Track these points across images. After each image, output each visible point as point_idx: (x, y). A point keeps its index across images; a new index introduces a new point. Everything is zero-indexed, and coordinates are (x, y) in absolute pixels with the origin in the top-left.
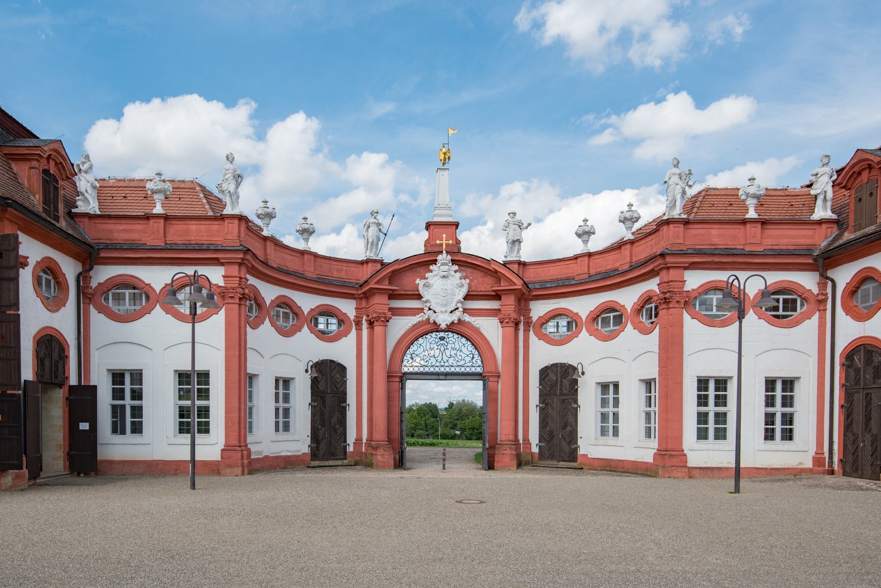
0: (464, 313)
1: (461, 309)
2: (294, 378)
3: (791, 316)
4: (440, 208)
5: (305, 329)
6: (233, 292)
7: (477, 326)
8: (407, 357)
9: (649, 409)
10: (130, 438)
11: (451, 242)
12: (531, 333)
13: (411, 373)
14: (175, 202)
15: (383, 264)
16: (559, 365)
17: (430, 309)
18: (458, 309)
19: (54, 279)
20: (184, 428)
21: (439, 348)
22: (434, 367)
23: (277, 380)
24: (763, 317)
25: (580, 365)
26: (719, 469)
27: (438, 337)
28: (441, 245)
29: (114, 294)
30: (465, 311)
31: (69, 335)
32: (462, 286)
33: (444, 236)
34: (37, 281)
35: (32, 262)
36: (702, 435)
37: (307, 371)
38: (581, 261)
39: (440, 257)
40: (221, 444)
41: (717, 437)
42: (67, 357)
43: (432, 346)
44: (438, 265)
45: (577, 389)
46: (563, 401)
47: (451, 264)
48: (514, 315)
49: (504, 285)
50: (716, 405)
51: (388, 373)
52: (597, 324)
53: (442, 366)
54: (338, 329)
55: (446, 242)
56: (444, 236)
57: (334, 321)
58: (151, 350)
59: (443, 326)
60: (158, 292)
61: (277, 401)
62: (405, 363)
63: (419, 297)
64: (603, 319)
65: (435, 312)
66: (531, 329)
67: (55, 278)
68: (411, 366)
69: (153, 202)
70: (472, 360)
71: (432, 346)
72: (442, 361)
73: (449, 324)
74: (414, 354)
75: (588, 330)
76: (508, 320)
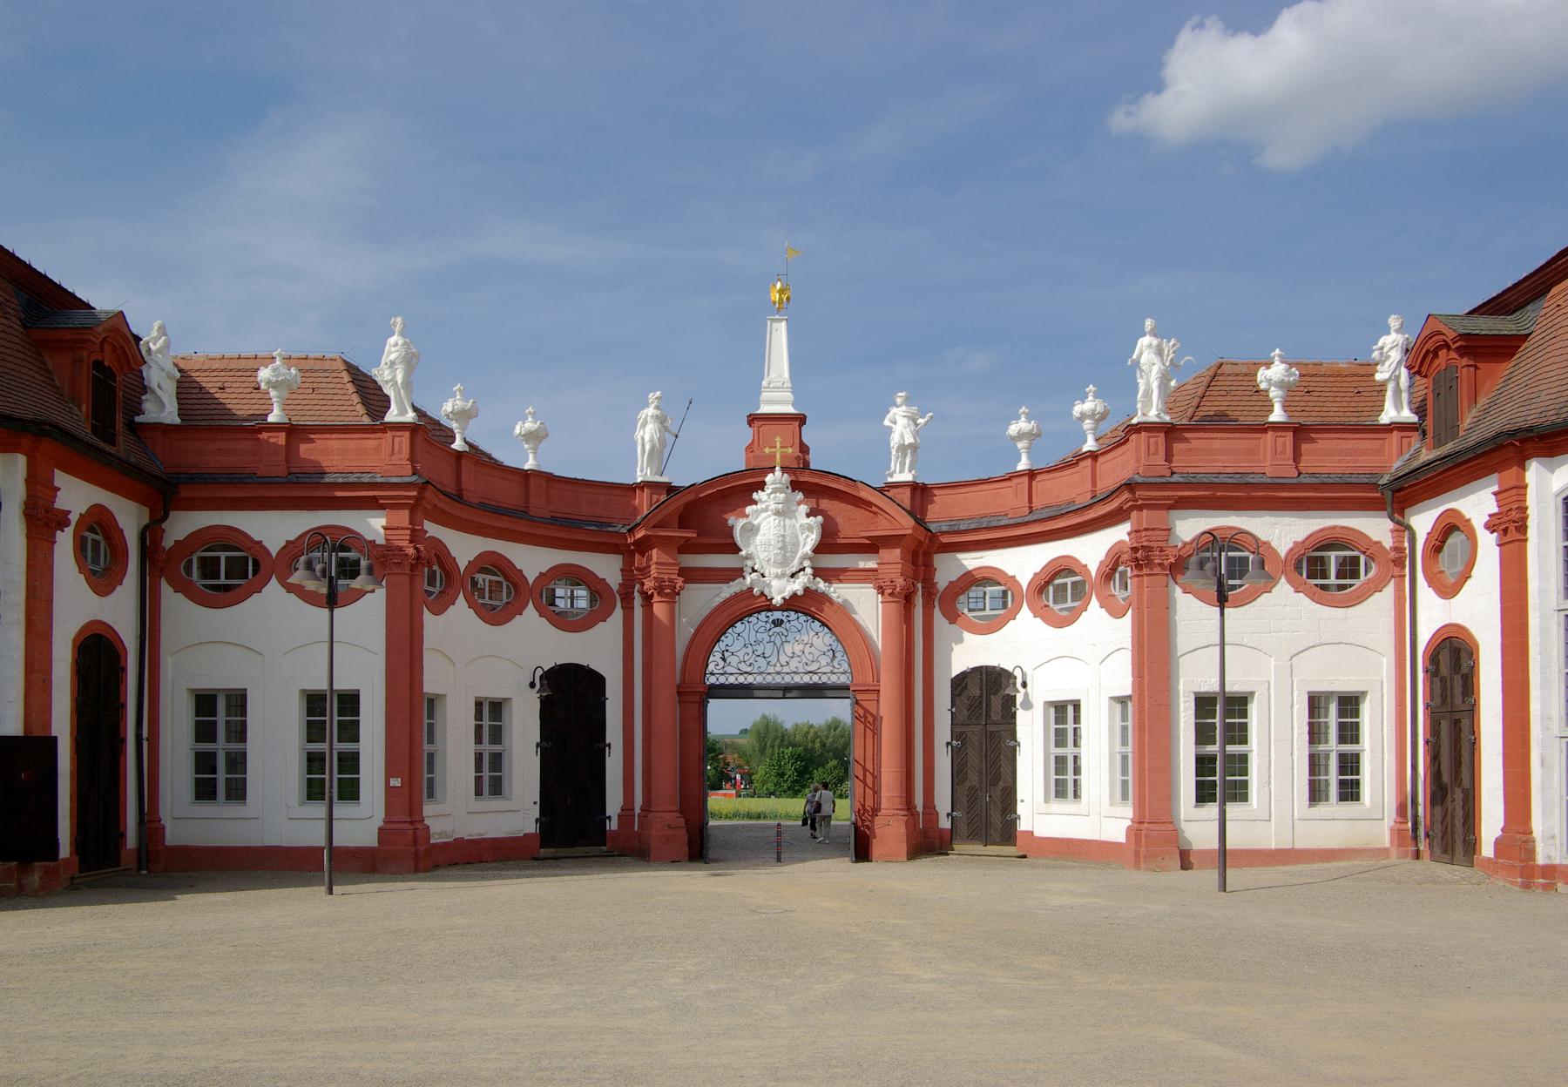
0: (815, 575)
1: (809, 571)
2: (511, 699)
3: (1351, 585)
4: (773, 388)
5: (530, 610)
6: (401, 555)
7: (840, 600)
8: (715, 658)
9: (1124, 749)
10: (221, 809)
12: (937, 613)
13: (722, 686)
14: (304, 396)
15: (670, 489)
16: (984, 671)
17: (754, 571)
18: (803, 569)
19: (105, 539)
20: (314, 791)
21: (773, 637)
22: (764, 675)
24: (1302, 590)
25: (1018, 670)
27: (770, 621)
28: (773, 456)
29: (203, 560)
30: (818, 573)
31: (128, 634)
33: (778, 439)
34: (80, 546)
35: (74, 518)
37: (532, 685)
38: (1018, 484)
39: (769, 478)
40: (379, 817)
42: (124, 670)
43: (760, 637)
44: (769, 491)
45: (1015, 712)
47: (790, 490)
49: (882, 528)
51: (678, 687)
52: (1048, 601)
53: (778, 673)
54: (591, 607)
56: (778, 439)
57: (582, 593)
58: (261, 654)
59: (778, 600)
60: (274, 556)
61: (479, 740)
62: (711, 667)
63: (735, 549)
65: (763, 576)
66: (936, 604)
67: (107, 538)
68: (722, 674)
69: (269, 402)
70: (832, 661)
71: (760, 637)
72: (778, 665)
73: (787, 598)
74: (727, 651)
76: (891, 591)
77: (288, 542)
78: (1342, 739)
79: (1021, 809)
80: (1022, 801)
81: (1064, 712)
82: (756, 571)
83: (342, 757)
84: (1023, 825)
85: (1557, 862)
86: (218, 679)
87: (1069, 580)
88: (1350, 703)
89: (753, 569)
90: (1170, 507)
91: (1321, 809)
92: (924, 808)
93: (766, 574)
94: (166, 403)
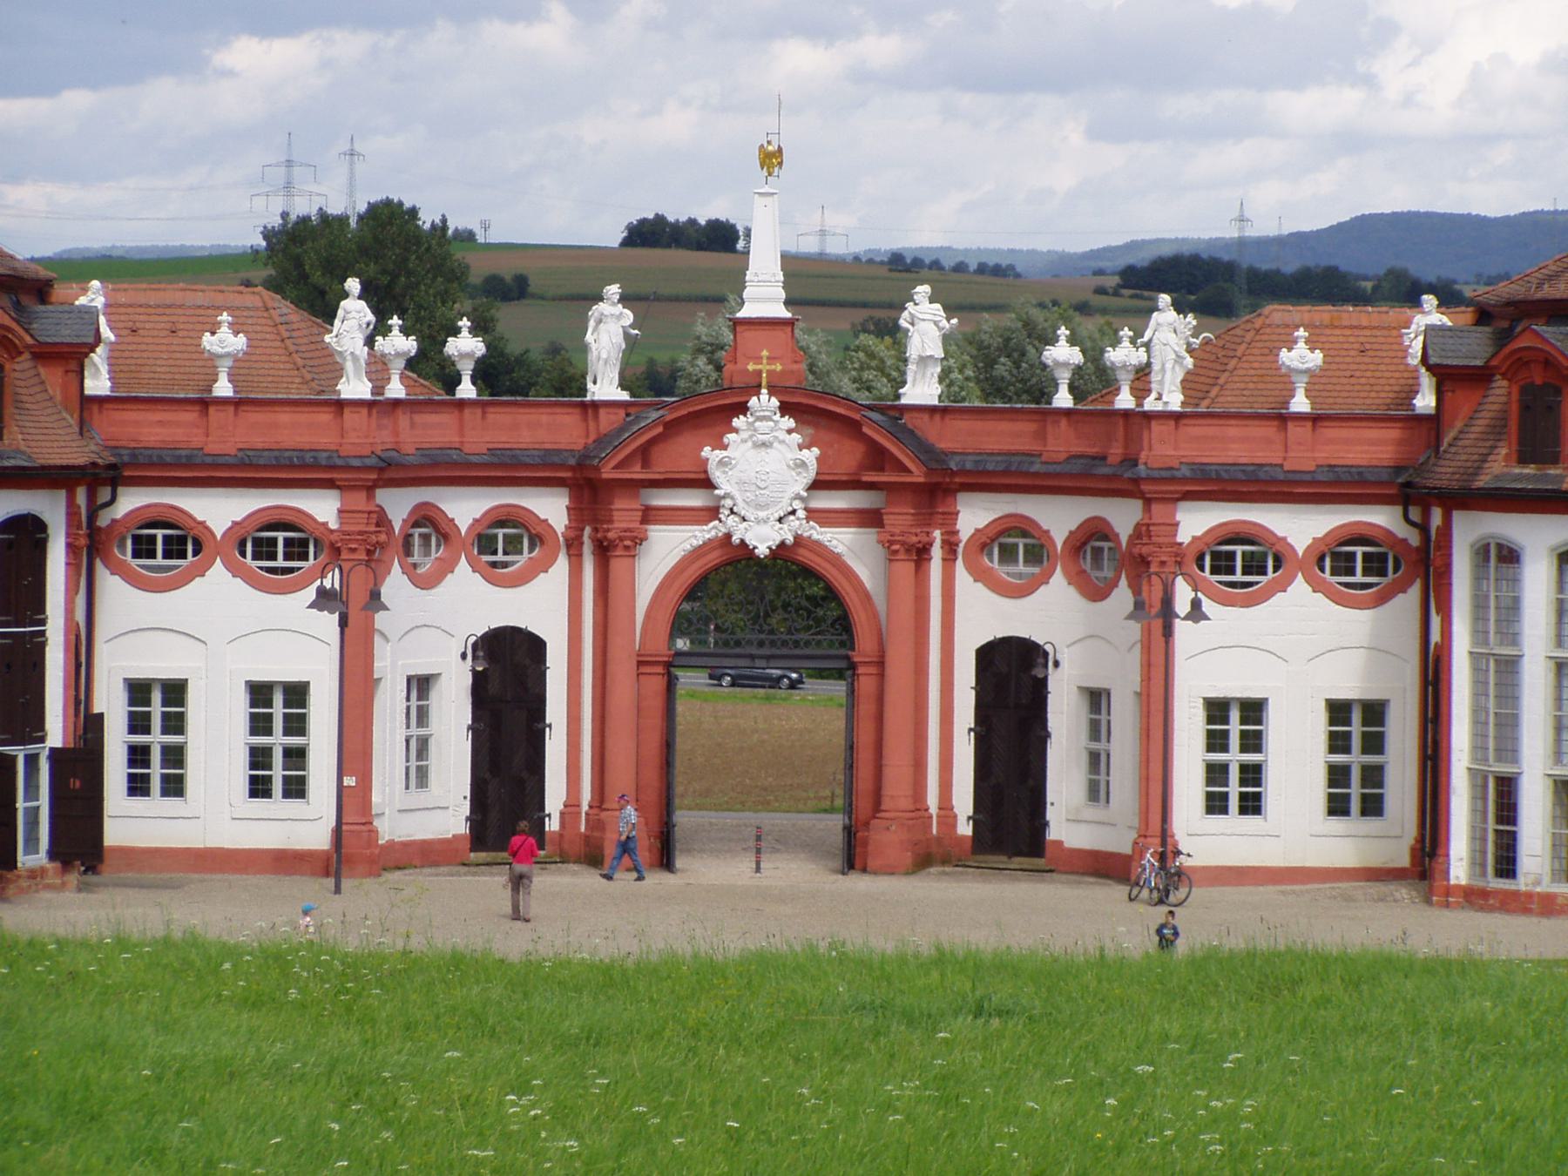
0: (808, 519)
1: (801, 514)
11: (779, 367)
18: (793, 512)
23: (409, 679)
28: (759, 373)
30: (813, 514)
33: (765, 353)
36: (1216, 804)
37: (464, 656)
41: (1243, 810)
47: (777, 417)
55: (768, 367)
60: (219, 537)
63: (707, 484)
65: (744, 519)
73: (774, 548)
75: (1066, 573)
77: (235, 524)
79: (1051, 814)
80: (1052, 804)
82: (735, 513)
86: (157, 665)
87: (1106, 545)
89: (731, 509)
90: (1178, 500)
91: (1338, 824)
92: (940, 809)
93: (748, 515)
94: (102, 369)
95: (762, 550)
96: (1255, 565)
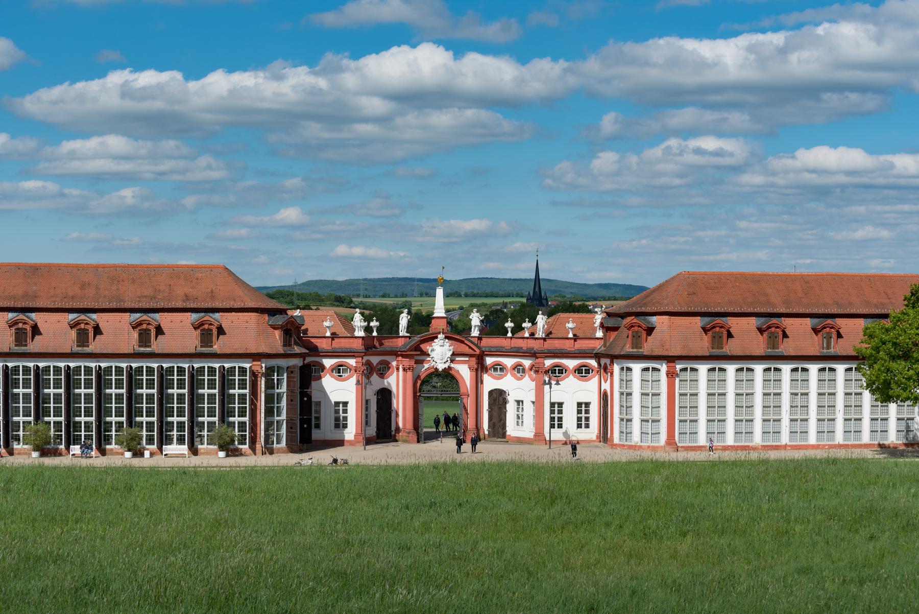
1: (449, 361)
18: (447, 361)
26: (559, 441)
32: (450, 350)
37: (375, 395)
39: (439, 336)
40: (354, 432)
41: (558, 427)
46: (500, 408)
48: (476, 366)
50: (558, 413)
64: (518, 369)
75: (511, 374)
78: (586, 413)
79: (507, 429)
81: (519, 402)
83: (343, 417)
84: (508, 433)
85: (617, 443)
87: (521, 368)
88: (587, 404)
95: (440, 370)
96: (561, 372)
